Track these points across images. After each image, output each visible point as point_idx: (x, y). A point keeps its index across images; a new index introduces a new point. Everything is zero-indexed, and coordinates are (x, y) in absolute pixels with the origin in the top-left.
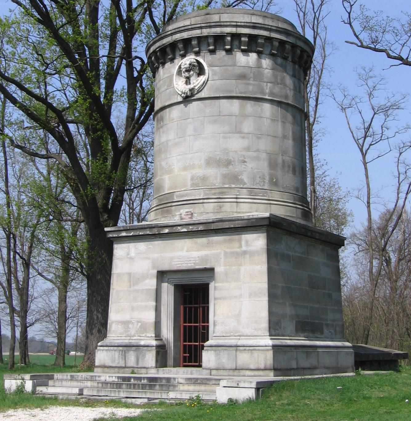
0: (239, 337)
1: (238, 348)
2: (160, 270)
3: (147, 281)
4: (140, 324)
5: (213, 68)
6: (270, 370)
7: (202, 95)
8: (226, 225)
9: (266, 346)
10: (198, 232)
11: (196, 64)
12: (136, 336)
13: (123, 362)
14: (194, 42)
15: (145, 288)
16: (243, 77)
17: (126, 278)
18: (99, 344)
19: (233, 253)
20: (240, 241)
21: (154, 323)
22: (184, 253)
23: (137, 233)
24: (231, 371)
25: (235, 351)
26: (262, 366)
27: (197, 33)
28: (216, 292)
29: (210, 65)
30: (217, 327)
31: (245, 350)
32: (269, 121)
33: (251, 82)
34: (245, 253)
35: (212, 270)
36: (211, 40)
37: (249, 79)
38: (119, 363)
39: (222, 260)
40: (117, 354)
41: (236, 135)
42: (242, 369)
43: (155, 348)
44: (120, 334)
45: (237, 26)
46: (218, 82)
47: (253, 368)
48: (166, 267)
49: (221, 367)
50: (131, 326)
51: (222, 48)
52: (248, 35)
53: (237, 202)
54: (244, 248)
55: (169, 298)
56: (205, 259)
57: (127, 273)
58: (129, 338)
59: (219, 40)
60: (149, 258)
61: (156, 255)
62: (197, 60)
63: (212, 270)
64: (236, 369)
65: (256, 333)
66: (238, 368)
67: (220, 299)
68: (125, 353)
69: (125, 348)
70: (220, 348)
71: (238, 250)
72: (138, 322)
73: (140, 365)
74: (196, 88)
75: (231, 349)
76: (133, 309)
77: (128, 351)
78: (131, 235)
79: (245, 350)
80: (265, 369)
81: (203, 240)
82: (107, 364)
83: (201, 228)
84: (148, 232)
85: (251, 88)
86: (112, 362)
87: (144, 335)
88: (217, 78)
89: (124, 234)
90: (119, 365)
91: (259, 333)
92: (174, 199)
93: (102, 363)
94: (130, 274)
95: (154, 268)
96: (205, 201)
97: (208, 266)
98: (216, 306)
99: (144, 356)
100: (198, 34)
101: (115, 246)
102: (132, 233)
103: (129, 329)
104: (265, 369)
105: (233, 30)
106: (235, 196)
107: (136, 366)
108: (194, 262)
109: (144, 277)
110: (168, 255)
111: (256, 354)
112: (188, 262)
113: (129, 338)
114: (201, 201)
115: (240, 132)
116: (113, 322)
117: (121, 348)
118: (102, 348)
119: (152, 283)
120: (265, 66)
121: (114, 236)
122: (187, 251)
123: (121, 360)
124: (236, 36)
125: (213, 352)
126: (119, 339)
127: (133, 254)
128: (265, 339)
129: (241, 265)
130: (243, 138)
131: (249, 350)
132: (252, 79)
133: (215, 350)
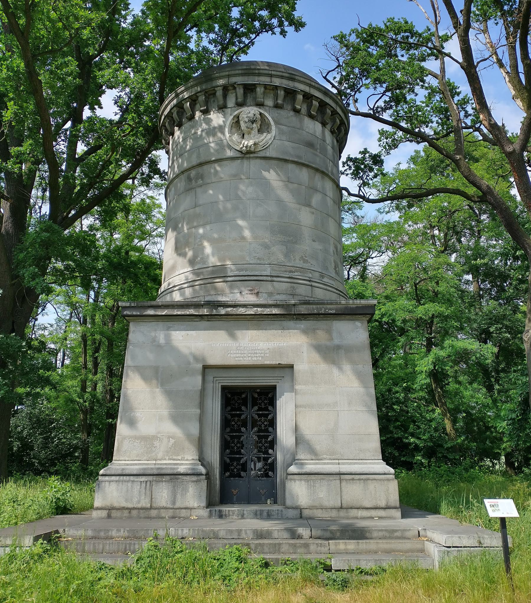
0: (337, 461)
1: (341, 476)
3: (186, 379)
4: (172, 441)
5: (280, 126)
6: (395, 508)
7: (268, 154)
9: (385, 474)
10: (270, 316)
11: (259, 116)
12: (165, 459)
13: (148, 500)
14: (260, 90)
16: (310, 145)
18: (101, 472)
20: (329, 331)
21: (197, 440)
23: (176, 312)
24: (334, 511)
25: (338, 482)
26: (383, 504)
27: (265, 80)
28: (297, 396)
29: (277, 123)
31: (353, 479)
32: (332, 202)
33: (318, 153)
34: (338, 347)
35: (291, 367)
36: (281, 93)
37: (316, 150)
38: (139, 502)
39: (305, 354)
41: (308, 209)
42: (351, 508)
43: (204, 477)
44: (137, 457)
45: (310, 86)
46: (287, 143)
47: (369, 507)
49: (317, 504)
50: (157, 443)
51: (290, 107)
52: (319, 100)
53: (311, 286)
54: (336, 342)
55: (214, 404)
58: (154, 462)
59: (290, 94)
62: (261, 114)
63: (291, 367)
64: (341, 508)
66: (344, 505)
67: (304, 406)
68: (151, 485)
69: (150, 478)
70: (313, 477)
71: (328, 343)
72: (169, 437)
73: (178, 505)
74: (260, 144)
75: (331, 477)
78: (164, 314)
79: (353, 479)
82: (116, 505)
83: (275, 311)
85: (318, 159)
86: (126, 501)
87: (180, 458)
88: (284, 138)
89: (151, 312)
90: (139, 506)
92: (227, 273)
93: (107, 503)
96: (275, 279)
97: (284, 361)
98: (298, 416)
99: (185, 490)
100: (267, 82)
101: (132, 327)
102: (166, 311)
103: (154, 449)
105: (307, 89)
106: (308, 279)
107: (171, 507)
108: (263, 355)
111: (372, 486)
112: (252, 355)
113: (154, 462)
114: (269, 278)
115: (309, 205)
116: (124, 438)
117: (143, 479)
118: (107, 478)
120: (328, 142)
121: (134, 313)
123: (143, 497)
124: (308, 97)
125: (303, 482)
126: (136, 464)
128: (378, 463)
130: (313, 213)
131: (359, 479)
132: (318, 151)
133: (307, 481)
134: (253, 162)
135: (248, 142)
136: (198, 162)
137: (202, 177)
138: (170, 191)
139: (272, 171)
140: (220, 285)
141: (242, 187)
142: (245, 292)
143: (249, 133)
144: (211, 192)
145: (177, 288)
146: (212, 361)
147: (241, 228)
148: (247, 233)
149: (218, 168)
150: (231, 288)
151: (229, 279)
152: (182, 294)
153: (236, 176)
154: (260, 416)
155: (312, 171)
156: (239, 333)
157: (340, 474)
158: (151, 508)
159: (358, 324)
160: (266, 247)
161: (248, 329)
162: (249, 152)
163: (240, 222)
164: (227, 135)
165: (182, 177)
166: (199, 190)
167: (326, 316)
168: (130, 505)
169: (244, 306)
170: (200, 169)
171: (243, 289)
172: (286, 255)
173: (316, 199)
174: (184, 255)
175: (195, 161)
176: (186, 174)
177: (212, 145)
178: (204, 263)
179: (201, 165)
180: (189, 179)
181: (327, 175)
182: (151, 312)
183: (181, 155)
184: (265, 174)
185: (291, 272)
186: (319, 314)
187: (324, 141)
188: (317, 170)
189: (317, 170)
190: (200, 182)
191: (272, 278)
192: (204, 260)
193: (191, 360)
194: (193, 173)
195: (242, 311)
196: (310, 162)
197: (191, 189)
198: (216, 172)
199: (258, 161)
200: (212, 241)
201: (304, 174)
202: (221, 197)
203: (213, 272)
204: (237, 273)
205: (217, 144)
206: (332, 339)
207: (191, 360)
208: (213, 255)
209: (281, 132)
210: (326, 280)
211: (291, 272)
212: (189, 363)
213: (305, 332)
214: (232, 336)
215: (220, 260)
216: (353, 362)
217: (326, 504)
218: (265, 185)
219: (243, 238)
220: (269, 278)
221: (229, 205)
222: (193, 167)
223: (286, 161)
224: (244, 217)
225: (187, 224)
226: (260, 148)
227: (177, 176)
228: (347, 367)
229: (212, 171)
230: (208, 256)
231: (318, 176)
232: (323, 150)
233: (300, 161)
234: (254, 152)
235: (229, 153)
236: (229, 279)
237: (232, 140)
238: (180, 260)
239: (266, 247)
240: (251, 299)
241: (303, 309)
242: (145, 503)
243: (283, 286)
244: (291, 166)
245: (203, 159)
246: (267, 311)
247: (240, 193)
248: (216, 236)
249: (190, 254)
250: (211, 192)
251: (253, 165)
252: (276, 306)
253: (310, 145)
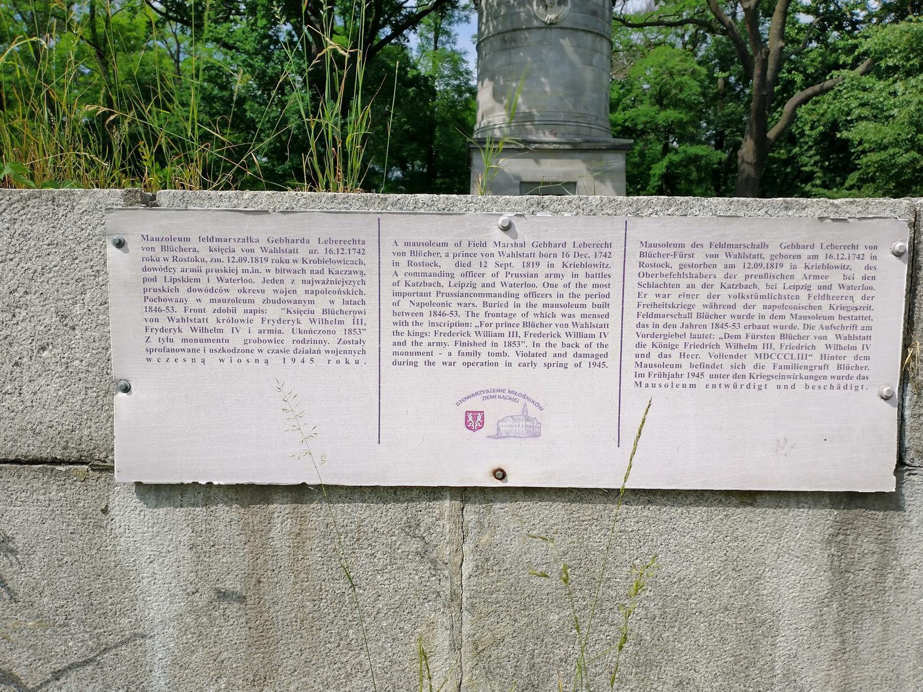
7: (564, 25)
8: (592, 146)
16: (594, 13)
35: (575, 183)
53: (590, 127)
63: (575, 183)
83: (567, 147)
96: (567, 123)
97: (571, 180)
114: (563, 123)
115: (591, 65)
130: (593, 70)
134: (554, 31)
135: (550, 17)
136: (512, 28)
137: (515, 40)
138: (485, 45)
139: (567, 39)
140: (529, 126)
141: (544, 51)
142: (547, 133)
143: (552, 7)
144: (522, 54)
145: (497, 126)
146: (525, 179)
147: (543, 84)
148: (548, 89)
149: (527, 35)
150: (537, 130)
151: (536, 123)
152: (501, 132)
153: (540, 42)
155: (594, 35)
156: (543, 161)
159: (619, 155)
160: (561, 99)
161: (548, 158)
162: (551, 24)
163: (543, 80)
164: (535, 8)
165: (499, 37)
166: (512, 51)
167: (600, 150)
169: (548, 143)
170: (513, 34)
171: (546, 131)
172: (575, 105)
173: (596, 59)
174: (501, 102)
175: (509, 27)
176: (501, 35)
177: (522, 14)
178: (518, 109)
179: (514, 30)
180: (504, 41)
181: (605, 37)
183: (496, 18)
184: (562, 41)
185: (577, 117)
186: (595, 149)
187: (604, 7)
188: (598, 34)
189: (598, 34)
190: (513, 44)
191: (565, 122)
192: (517, 107)
193: (513, 178)
194: (507, 36)
195: (546, 146)
196: (594, 28)
197: (506, 49)
198: (526, 38)
199: (558, 30)
200: (523, 94)
201: (589, 38)
202: (529, 59)
203: (524, 117)
204: (541, 119)
205: (526, 15)
207: (513, 178)
208: (524, 103)
210: (599, 122)
211: (577, 117)
212: (511, 180)
213: (584, 161)
214: (537, 162)
215: (529, 108)
216: (612, 180)
218: (561, 50)
219: (545, 92)
220: (563, 123)
221: (535, 66)
222: (507, 32)
223: (577, 30)
224: (546, 76)
225: (503, 78)
226: (559, 20)
227: (493, 36)
228: (609, 184)
229: (523, 37)
230: (519, 105)
231: (598, 39)
232: (603, 14)
233: (587, 29)
234: (555, 24)
235: (536, 23)
236: (536, 123)
237: (538, 13)
238: (498, 105)
239: (561, 99)
240: (552, 139)
241: (585, 146)
243: (572, 128)
244: (581, 34)
245: (516, 26)
246: (562, 147)
247: (543, 56)
248: (525, 89)
249: (506, 102)
250: (522, 54)
251: (552, 34)
252: (568, 143)
253: (594, 13)
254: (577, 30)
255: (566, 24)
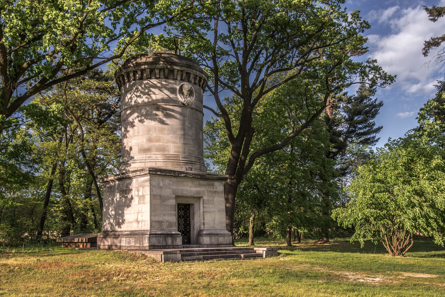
2: (177, 195)
3: (170, 201)
15: (169, 204)
17: (158, 197)
19: (210, 191)
22: (188, 188)
26: (228, 243)
30: (205, 226)
40: (161, 239)
48: (180, 194)
50: (163, 224)
54: (215, 190)
56: (198, 192)
57: (159, 195)
60: (171, 189)
61: (174, 187)
65: (221, 229)
71: (213, 190)
72: (167, 222)
73: (174, 244)
76: (164, 215)
77: (168, 237)
80: (229, 244)
81: (197, 182)
82: (156, 245)
84: (173, 174)
89: (159, 173)
91: (223, 228)
94: (160, 196)
95: (173, 194)
99: (176, 240)
104: (229, 244)
109: (169, 198)
110: (180, 188)
111: (226, 238)
117: (163, 236)
119: (173, 202)
122: (190, 187)
127: (161, 185)
129: (214, 197)
154: (184, 214)
157: (217, 234)
158: (166, 245)
168: (160, 245)
182: (159, 173)
206: (214, 188)
209: (196, 97)
217: (215, 243)
223: (197, 110)
242: (164, 244)
254: (197, 110)
255: (193, 106)
